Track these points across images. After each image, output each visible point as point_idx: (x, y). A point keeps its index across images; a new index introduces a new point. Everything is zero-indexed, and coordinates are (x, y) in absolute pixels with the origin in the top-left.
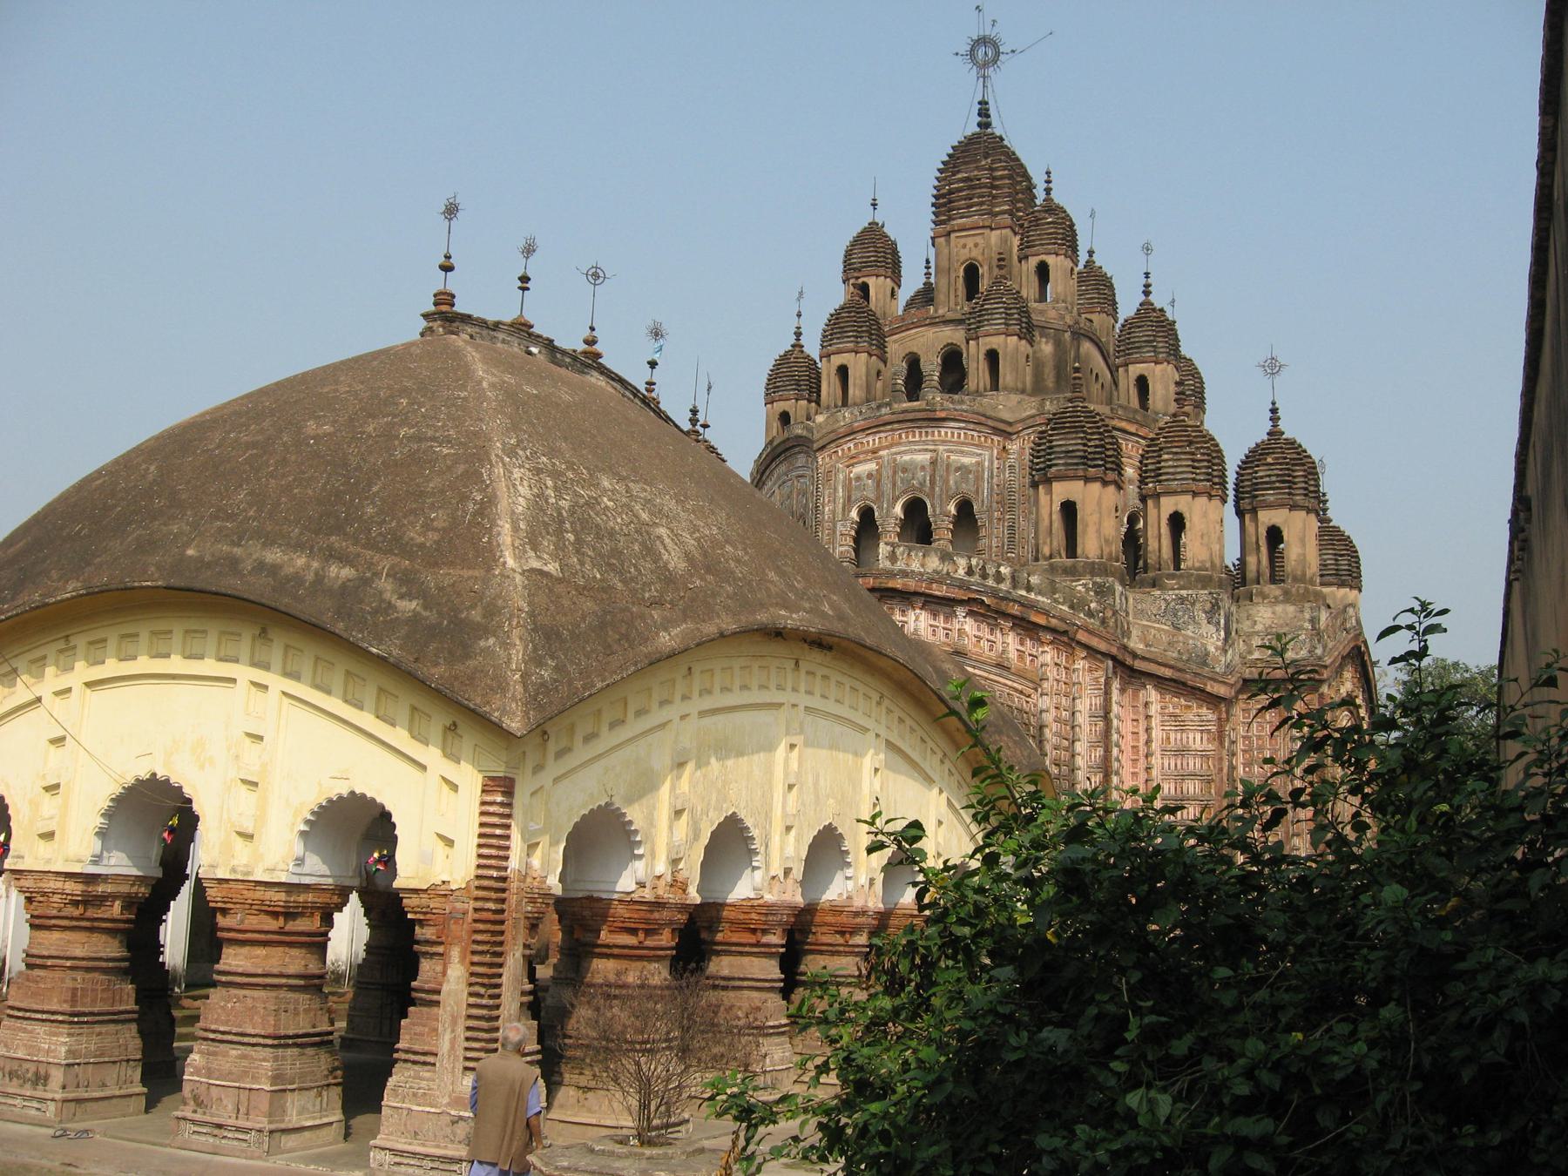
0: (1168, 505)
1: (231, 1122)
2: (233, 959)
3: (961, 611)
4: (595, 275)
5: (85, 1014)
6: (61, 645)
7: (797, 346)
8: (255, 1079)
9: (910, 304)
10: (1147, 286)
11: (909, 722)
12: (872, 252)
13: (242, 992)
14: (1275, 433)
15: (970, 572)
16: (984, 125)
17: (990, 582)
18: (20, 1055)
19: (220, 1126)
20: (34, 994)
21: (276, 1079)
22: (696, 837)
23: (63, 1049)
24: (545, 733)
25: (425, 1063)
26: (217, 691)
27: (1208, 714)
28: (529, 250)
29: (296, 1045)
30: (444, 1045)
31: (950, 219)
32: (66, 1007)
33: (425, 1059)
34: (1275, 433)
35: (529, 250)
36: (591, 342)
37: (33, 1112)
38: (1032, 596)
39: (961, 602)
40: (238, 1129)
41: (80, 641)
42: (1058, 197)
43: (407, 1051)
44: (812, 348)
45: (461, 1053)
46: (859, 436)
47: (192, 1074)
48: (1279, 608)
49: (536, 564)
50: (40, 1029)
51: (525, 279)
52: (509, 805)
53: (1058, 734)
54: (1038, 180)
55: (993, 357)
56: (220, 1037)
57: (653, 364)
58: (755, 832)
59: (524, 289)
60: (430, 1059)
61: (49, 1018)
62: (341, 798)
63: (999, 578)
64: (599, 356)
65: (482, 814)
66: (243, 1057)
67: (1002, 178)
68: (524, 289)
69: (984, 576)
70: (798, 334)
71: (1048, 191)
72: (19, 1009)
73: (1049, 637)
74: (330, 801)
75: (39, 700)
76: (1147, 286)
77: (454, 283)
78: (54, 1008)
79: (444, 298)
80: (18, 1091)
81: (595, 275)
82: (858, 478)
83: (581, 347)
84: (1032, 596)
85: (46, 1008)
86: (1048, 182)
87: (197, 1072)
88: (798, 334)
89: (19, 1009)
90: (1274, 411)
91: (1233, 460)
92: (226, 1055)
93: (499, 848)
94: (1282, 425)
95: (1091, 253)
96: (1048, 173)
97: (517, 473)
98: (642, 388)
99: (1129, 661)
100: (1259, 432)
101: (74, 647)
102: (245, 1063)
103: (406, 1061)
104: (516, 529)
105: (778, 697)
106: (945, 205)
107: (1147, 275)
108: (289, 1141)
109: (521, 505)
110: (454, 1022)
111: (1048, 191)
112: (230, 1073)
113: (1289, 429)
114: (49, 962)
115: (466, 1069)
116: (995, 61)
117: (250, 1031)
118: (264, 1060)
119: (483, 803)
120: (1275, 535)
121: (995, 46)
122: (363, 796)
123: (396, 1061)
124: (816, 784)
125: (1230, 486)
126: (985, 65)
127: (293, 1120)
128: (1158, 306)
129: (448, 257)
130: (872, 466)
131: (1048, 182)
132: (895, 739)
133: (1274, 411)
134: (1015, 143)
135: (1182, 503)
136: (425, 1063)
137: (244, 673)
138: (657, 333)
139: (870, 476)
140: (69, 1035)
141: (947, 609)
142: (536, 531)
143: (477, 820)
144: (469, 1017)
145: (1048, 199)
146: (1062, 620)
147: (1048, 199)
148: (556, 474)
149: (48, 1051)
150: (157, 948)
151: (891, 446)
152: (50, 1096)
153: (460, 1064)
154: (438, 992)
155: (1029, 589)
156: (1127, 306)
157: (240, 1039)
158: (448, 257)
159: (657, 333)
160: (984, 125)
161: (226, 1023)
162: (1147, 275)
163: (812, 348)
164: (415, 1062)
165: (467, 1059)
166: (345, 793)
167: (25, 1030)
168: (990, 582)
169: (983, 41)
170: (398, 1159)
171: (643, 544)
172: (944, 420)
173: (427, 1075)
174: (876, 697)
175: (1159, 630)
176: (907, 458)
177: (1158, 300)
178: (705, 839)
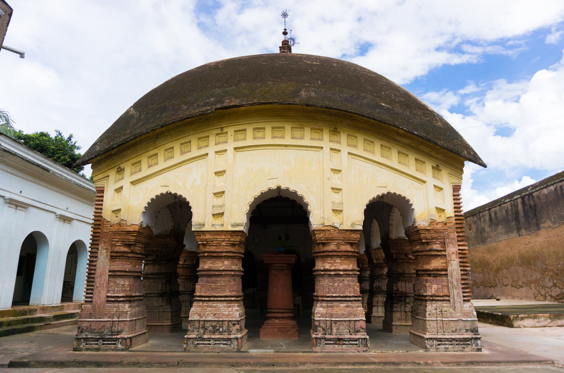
1: (348, 336)
6: (219, 131)
13: (341, 279)
18: (210, 319)
19: (340, 340)
20: (213, 289)
23: (238, 313)
25: (446, 300)
26: (311, 153)
32: (234, 293)
33: (446, 298)
37: (222, 346)
40: (351, 340)
45: (461, 295)
47: (319, 317)
50: (220, 305)
56: (334, 299)
60: (447, 298)
61: (228, 300)
66: (347, 307)
72: (205, 297)
75: (207, 154)
78: (228, 294)
80: (212, 337)
85: (225, 294)
87: (322, 316)
89: (205, 297)
92: (338, 306)
101: (227, 133)
102: (349, 309)
103: (432, 300)
110: (457, 281)
112: (343, 315)
117: (348, 294)
118: (358, 307)
119: (454, 195)
136: (443, 300)
140: (238, 306)
143: (453, 202)
149: (228, 315)
152: (233, 336)
153: (462, 299)
157: (344, 299)
161: (335, 293)
164: (438, 300)
165: (464, 296)
167: (211, 307)
170: (439, 343)
173: (446, 305)
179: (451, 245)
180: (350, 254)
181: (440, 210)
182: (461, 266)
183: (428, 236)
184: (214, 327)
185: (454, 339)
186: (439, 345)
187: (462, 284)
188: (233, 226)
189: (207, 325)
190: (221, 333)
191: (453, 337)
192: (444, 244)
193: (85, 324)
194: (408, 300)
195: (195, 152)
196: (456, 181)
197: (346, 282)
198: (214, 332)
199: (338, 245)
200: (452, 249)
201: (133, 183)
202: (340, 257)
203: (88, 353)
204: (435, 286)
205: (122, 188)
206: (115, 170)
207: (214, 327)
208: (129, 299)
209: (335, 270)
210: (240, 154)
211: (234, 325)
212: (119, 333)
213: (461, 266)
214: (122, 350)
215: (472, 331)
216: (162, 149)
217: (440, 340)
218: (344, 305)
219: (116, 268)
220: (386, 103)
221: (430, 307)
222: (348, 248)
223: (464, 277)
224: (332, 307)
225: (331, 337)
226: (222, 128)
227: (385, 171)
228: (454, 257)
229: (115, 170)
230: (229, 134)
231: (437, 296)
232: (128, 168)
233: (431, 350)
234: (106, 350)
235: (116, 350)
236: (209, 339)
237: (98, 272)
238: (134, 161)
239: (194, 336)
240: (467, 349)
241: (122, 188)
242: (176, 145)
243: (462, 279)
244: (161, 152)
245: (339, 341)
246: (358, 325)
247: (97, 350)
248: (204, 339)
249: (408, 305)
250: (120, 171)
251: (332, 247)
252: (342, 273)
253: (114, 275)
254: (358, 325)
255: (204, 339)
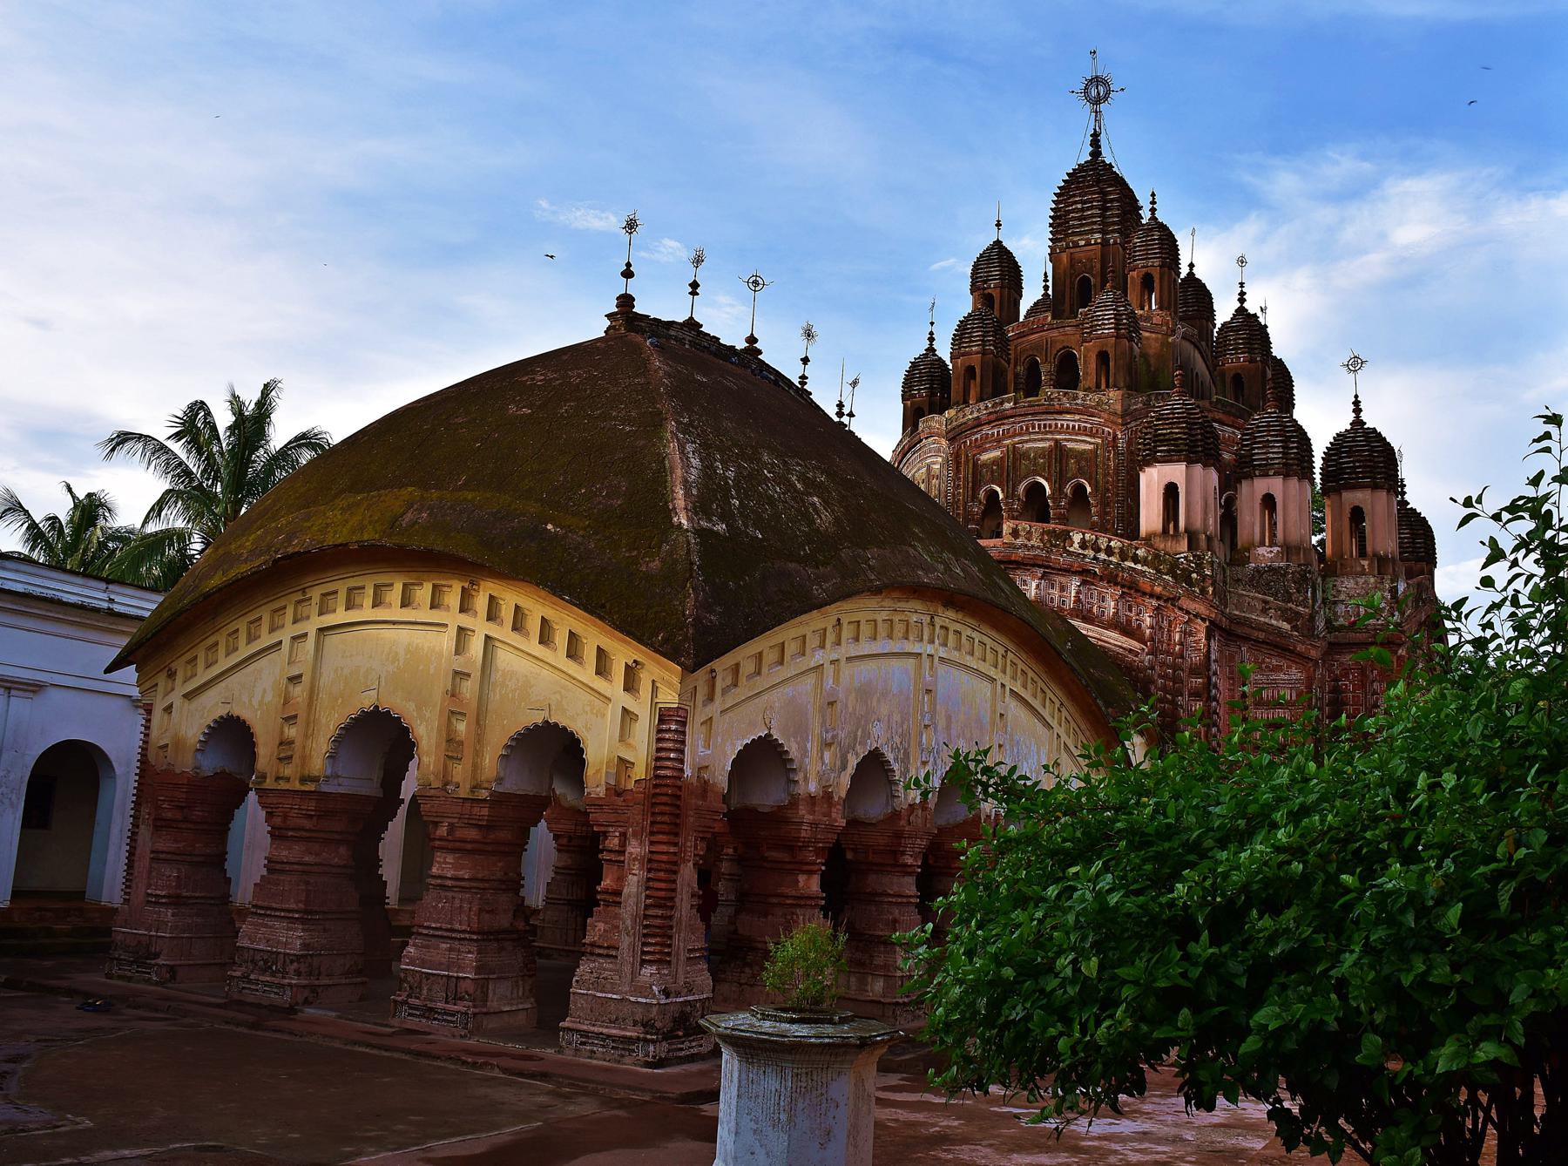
0: (1262, 486)
2: (444, 865)
3: (1074, 584)
4: (756, 283)
5: (317, 913)
7: (931, 350)
8: (461, 969)
9: (1030, 313)
10: (1242, 294)
11: (1030, 674)
12: (997, 270)
13: (450, 894)
14: (1358, 423)
15: (1083, 545)
16: (1096, 153)
17: (1102, 556)
19: (431, 1009)
21: (478, 970)
22: (844, 767)
24: (713, 671)
25: (608, 956)
27: (1296, 674)
28: (698, 261)
29: (497, 940)
30: (625, 942)
31: (1067, 235)
32: (301, 906)
33: (609, 951)
34: (1358, 423)
35: (698, 261)
36: (752, 340)
38: (1139, 567)
39: (1075, 573)
41: (315, 594)
42: (1161, 217)
43: (593, 945)
44: (944, 352)
46: (986, 430)
48: (1361, 581)
49: (704, 524)
51: (694, 285)
52: (684, 733)
53: (1164, 689)
54: (1144, 200)
55: (1103, 357)
57: (805, 361)
58: (896, 767)
59: (694, 293)
62: (536, 726)
63: (1109, 551)
64: (760, 352)
65: (659, 740)
67: (1112, 201)
68: (694, 293)
69: (1097, 550)
70: (931, 339)
71: (1153, 210)
72: (262, 908)
73: (1154, 603)
74: (527, 729)
76: (1242, 294)
77: (633, 287)
78: (293, 906)
79: (626, 301)
81: (756, 283)
82: (984, 465)
83: (741, 345)
84: (1139, 567)
86: (1153, 203)
88: (931, 339)
89: (262, 908)
90: (1357, 403)
91: (1320, 445)
93: (673, 769)
94: (1363, 416)
95: (1191, 266)
96: (1153, 195)
97: (689, 448)
98: (796, 381)
99: (1225, 623)
100: (1344, 423)
103: (592, 954)
104: (687, 494)
105: (916, 648)
106: (1060, 223)
107: (1242, 285)
108: (492, 1023)
109: (694, 475)
111: (1153, 210)
113: (1370, 419)
114: (288, 867)
115: (643, 962)
116: (1106, 98)
117: (457, 926)
119: (659, 731)
120: (1357, 515)
121: (1105, 83)
122: (556, 725)
123: (583, 954)
124: (948, 727)
125: (1317, 471)
126: (1097, 101)
127: (493, 1004)
128: (1251, 311)
129: (629, 265)
130: (997, 453)
131: (1153, 203)
132: (1018, 689)
133: (1357, 403)
134: (1122, 169)
135: (1275, 485)
136: (608, 956)
137: (454, 619)
138: (809, 334)
139: (995, 462)
141: (1063, 579)
142: (707, 499)
144: (646, 917)
145: (1153, 218)
146: (1166, 585)
147: (1153, 218)
148: (721, 450)
149: (286, 944)
150: (375, 863)
151: (1014, 435)
154: (618, 893)
155: (1136, 559)
156: (1224, 312)
157: (448, 935)
158: (629, 265)
159: (809, 334)
160: (1096, 153)
162: (1242, 285)
163: (944, 352)
166: (540, 721)
167: (266, 926)
168: (1102, 556)
169: (1097, 81)
171: (798, 511)
172: (1060, 413)
174: (1001, 651)
175: (1253, 598)
176: (1027, 446)
177: (1252, 307)
178: (851, 770)
179: (634, 842)
180: (469, 846)
181: (624, 764)
182: (648, 888)
183: (602, 818)
184: (266, 962)
185: (609, 1036)
186: (583, 1043)
187: (646, 927)
188: (303, 780)
189: (258, 957)
190: (273, 974)
191: (605, 1031)
192: (623, 835)
193: (119, 937)
194: (750, 958)
195: (266, 640)
196: (669, 697)
197: (457, 903)
198: (264, 971)
199: (452, 827)
200: (635, 848)
201: (189, 696)
202: (453, 850)
203: (120, 983)
204: (601, 926)
205: (171, 706)
206: (163, 675)
207: (266, 962)
208: (176, 901)
209: (440, 877)
210: (333, 640)
211: (292, 962)
212: (157, 956)
213: (648, 888)
214: (157, 984)
215: (644, 1026)
216: (225, 632)
217: (584, 1034)
218: (444, 946)
219: (160, 846)
220: (555, 526)
221: (584, 968)
222: (473, 834)
223: (650, 912)
224: (427, 947)
225: (417, 1002)
226: (304, 591)
227: (546, 673)
228: (636, 868)
229: (163, 675)
230: (313, 601)
231: (601, 947)
232: (180, 666)
233: (567, 1051)
234: (138, 982)
235: (148, 981)
236: (257, 982)
237: (138, 851)
238: (188, 656)
239: (238, 974)
240: (627, 1060)
241: (171, 706)
242: (242, 625)
243: (646, 917)
244: (221, 637)
245: (428, 1012)
246: (463, 985)
247: (130, 979)
248: (250, 981)
249: (747, 970)
250: (172, 675)
251: (443, 831)
252: (449, 883)
253: (157, 857)
254: (463, 985)
255: (250, 981)
